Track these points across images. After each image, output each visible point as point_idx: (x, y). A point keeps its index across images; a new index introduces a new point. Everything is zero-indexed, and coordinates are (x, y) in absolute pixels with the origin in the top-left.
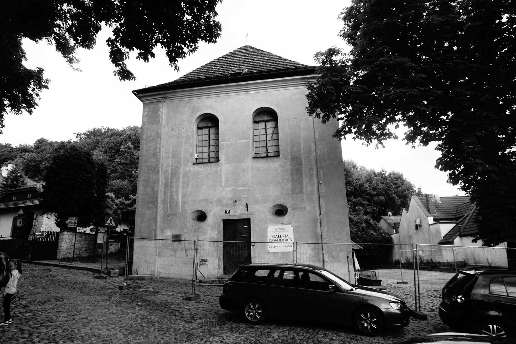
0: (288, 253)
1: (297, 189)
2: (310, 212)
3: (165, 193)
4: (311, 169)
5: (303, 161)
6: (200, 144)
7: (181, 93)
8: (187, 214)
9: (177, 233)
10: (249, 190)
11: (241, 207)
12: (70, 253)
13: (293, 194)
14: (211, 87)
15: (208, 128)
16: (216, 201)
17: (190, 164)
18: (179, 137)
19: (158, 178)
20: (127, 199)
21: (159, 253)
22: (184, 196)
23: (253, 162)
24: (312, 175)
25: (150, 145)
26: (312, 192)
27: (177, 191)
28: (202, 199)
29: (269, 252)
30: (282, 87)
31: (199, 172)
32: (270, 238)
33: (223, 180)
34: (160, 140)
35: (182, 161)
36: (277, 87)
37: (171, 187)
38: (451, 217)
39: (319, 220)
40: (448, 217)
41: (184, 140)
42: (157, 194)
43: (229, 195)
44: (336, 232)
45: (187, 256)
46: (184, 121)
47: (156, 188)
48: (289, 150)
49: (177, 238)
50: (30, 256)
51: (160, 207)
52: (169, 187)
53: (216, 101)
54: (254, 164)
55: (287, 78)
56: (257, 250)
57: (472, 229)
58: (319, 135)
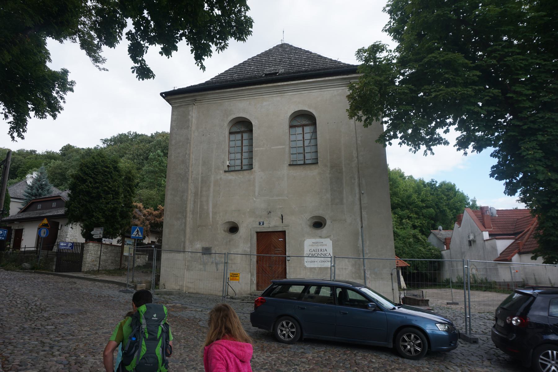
3: (195, 202)
5: (344, 170)
6: (232, 150)
7: (211, 95)
9: (207, 245)
12: (95, 265)
14: (244, 88)
17: (221, 172)
20: (156, 209)
29: (305, 267)
32: (306, 251)
33: (257, 189)
34: (190, 146)
36: (315, 88)
38: (509, 232)
39: (360, 234)
40: (505, 233)
45: (217, 270)
49: (207, 251)
50: (54, 267)
55: (327, 78)
57: (532, 246)
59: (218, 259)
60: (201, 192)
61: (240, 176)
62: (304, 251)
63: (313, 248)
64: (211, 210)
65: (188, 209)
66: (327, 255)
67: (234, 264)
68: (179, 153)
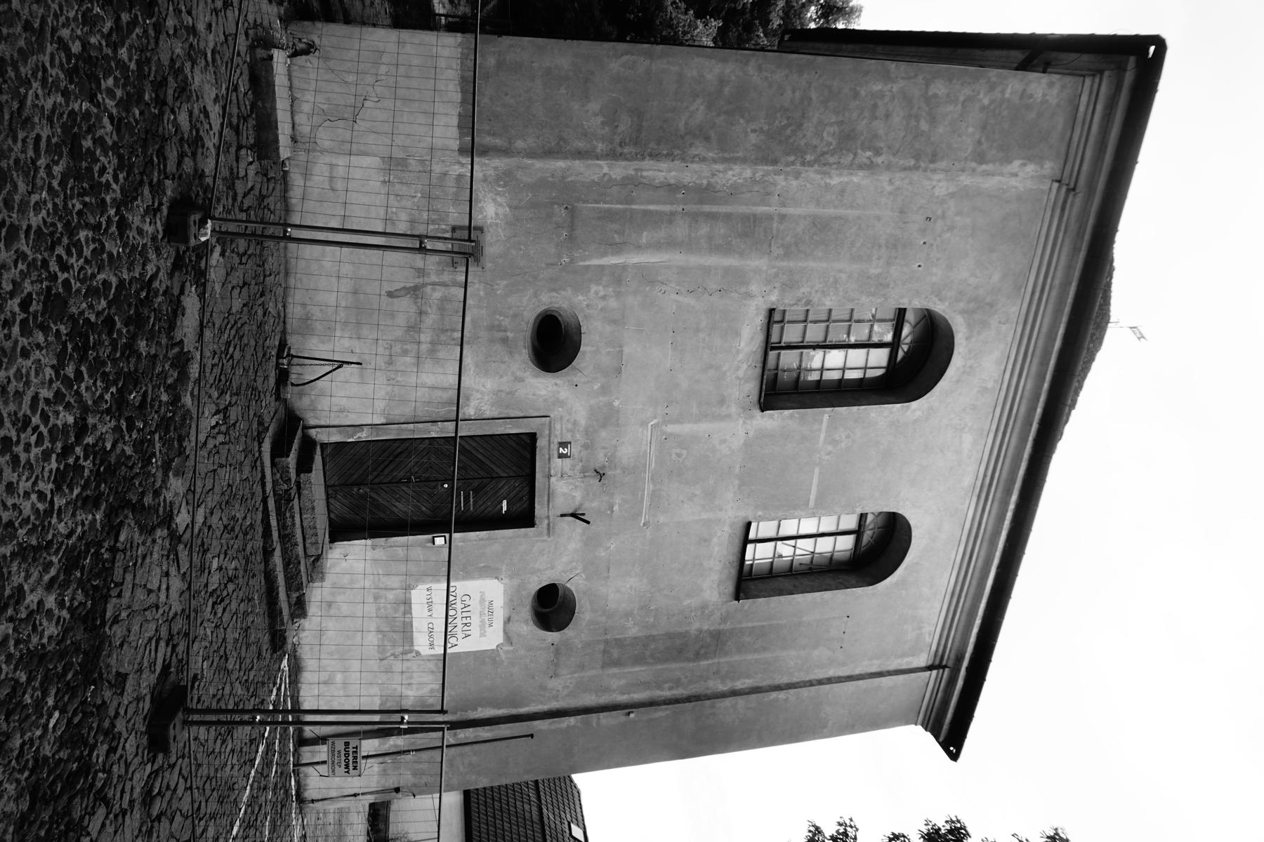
0: (410, 640)
1: (615, 652)
2: (543, 687)
3: (673, 189)
4: (677, 683)
5: (704, 663)
9: (493, 245)
11: (578, 495)
13: (607, 642)
14: (1046, 386)
16: (610, 404)
17: (773, 298)
18: (897, 245)
19: (744, 161)
21: (402, 163)
22: (647, 276)
23: (731, 526)
24: (659, 687)
26: (607, 690)
28: (626, 350)
29: (408, 588)
30: (956, 595)
31: (738, 334)
32: (459, 586)
33: (686, 428)
35: (792, 264)
37: (695, 217)
39: (514, 711)
41: (873, 271)
42: (670, 156)
43: (626, 453)
44: (474, 759)
45: (391, 295)
47: (699, 149)
48: (750, 625)
49: (466, 246)
51: (610, 167)
53: (984, 390)
54: (727, 529)
55: (978, 622)
56: (417, 553)
58: (777, 700)
59: (438, 294)
60: (712, 217)
61: (745, 366)
62: (464, 578)
63: (474, 604)
64: (635, 259)
65: (647, 163)
67: (418, 364)
68: (887, 116)
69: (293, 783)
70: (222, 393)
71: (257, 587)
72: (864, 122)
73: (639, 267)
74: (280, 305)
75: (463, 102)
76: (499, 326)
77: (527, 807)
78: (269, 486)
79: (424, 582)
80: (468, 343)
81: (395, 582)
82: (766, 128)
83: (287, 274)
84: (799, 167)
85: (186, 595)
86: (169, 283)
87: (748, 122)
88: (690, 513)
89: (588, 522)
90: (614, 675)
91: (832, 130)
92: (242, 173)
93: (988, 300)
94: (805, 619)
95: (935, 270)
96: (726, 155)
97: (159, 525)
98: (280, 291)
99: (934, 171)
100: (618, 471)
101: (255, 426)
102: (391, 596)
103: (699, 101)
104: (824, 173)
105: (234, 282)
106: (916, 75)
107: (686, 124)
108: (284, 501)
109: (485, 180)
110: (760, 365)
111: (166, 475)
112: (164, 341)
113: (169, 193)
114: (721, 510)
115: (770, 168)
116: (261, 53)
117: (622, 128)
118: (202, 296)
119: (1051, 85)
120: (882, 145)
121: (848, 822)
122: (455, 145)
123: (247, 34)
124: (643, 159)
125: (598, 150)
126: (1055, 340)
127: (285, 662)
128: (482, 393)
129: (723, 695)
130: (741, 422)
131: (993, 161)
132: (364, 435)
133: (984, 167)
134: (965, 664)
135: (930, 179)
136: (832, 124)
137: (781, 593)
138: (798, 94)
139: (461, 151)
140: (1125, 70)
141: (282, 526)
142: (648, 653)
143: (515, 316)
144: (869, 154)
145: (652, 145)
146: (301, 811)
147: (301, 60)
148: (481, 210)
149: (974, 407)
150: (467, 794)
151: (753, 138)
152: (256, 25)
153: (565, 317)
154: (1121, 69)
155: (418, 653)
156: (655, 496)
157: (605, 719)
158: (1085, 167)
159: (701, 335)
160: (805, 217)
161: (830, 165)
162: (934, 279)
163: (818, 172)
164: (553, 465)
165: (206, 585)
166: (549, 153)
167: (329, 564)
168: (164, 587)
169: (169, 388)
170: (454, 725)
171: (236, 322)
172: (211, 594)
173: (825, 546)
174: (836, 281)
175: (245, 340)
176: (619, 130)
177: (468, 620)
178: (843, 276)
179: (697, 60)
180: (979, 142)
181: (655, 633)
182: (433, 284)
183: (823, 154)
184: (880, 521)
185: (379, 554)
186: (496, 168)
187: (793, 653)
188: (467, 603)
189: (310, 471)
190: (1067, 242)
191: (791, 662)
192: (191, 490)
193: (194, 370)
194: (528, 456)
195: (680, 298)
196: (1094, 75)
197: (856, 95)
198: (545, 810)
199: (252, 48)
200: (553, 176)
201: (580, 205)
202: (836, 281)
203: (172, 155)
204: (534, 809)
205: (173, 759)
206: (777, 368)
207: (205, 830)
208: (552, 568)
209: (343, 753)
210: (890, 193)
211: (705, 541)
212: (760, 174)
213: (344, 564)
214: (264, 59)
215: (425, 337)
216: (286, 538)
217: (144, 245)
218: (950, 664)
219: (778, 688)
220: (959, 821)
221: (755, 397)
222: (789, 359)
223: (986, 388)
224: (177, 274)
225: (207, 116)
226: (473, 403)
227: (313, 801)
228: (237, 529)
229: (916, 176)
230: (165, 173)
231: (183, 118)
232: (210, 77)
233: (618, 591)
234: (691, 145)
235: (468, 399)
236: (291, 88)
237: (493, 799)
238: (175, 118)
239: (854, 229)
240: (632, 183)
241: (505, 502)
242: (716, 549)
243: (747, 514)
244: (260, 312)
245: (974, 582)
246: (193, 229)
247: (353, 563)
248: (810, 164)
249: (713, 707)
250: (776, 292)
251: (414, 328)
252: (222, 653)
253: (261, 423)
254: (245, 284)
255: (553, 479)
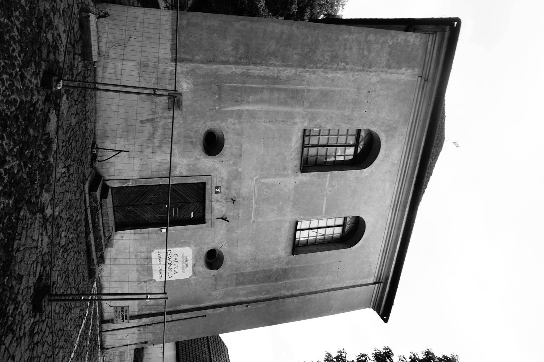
1: (242, 278)
4: (268, 292)
5: (279, 283)
7: (426, 110)
8: (219, 122)
9: (186, 102)
10: (251, 218)
11: (224, 210)
13: (237, 274)
14: (419, 162)
15: (356, 146)
16: (237, 170)
17: (306, 125)
18: (356, 103)
19: (292, 66)
21: (147, 66)
22: (252, 115)
24: (260, 294)
25: (355, 50)
27: (262, 101)
28: (244, 146)
29: (151, 251)
30: (385, 251)
31: (291, 140)
32: (173, 251)
33: (270, 180)
34: (358, 71)
35: (313, 110)
37: (272, 90)
39: (197, 306)
42: (261, 64)
43: (244, 191)
44: (180, 327)
45: (142, 122)
46: (378, 112)
47: (273, 61)
48: (299, 266)
51: (236, 68)
52: (272, 86)
53: (394, 164)
54: (288, 224)
55: (394, 262)
56: (154, 236)
60: (279, 90)
61: (294, 154)
63: (179, 258)
64: (247, 107)
65: (252, 67)
66: (170, 275)
68: (351, 49)
69: (99, 339)
70: (67, 159)
71: (82, 248)
72: (341, 51)
73: (248, 111)
74: (93, 126)
75: (173, 40)
76: (189, 136)
77: (204, 356)
78: (88, 204)
79: (157, 249)
80: (176, 143)
81: (144, 249)
82: (301, 52)
83: (96, 113)
84: (315, 69)
85: (50, 245)
86: (43, 107)
87: (293, 50)
88: (272, 217)
89: (228, 221)
90: (241, 289)
91: (328, 54)
92: (76, 65)
93: (394, 126)
94: (322, 263)
95: (372, 113)
96: (285, 64)
97: (38, 212)
98: (93, 120)
99: (371, 72)
100: (241, 199)
101: (81, 177)
102: (142, 255)
103: (273, 41)
104: (325, 72)
105: (72, 112)
106: (362, 32)
107: (267, 50)
108: (94, 211)
109: (182, 73)
110: (300, 153)
111: (41, 192)
112: (41, 131)
113: (43, 67)
114: (285, 216)
115: (303, 69)
116: (84, 14)
117: (240, 51)
118: (58, 115)
119: (416, 37)
120: (349, 60)
121: (342, 350)
122: (169, 57)
123: (78, 6)
124: (250, 65)
125: (231, 61)
126: (422, 142)
127: (95, 285)
128: (182, 165)
129: (288, 297)
130: (293, 177)
131: (394, 68)
132: (130, 184)
133: (391, 70)
134: (389, 281)
135: (369, 75)
136: (328, 52)
137: (311, 252)
138: (314, 39)
139: (172, 60)
140: (445, 31)
141: (94, 222)
142: (255, 279)
143: (196, 132)
144: (343, 64)
145: (253, 59)
146: (102, 353)
147: (102, 20)
148: (181, 86)
149: (390, 171)
150: (177, 344)
151: (296, 57)
152: (82, 3)
153: (217, 133)
154: (444, 31)
155: (155, 281)
156: (257, 210)
157: (237, 308)
158: (431, 71)
159: (275, 140)
160: (318, 91)
161: (328, 68)
162: (372, 117)
163: (323, 72)
164: (213, 197)
165: (59, 243)
166: (210, 62)
167: (115, 241)
168: (40, 239)
169: (43, 153)
170: (169, 313)
171: (73, 129)
172: (62, 247)
173: (329, 231)
174: (331, 118)
175: (77, 138)
176: (239, 52)
177: (177, 266)
178: (334, 115)
179: (272, 24)
180: (388, 60)
181: (258, 270)
182: (160, 118)
183: (325, 64)
184: (352, 221)
185: (137, 236)
186: (187, 68)
187: (317, 278)
188: (176, 258)
189: (106, 198)
190: (425, 102)
191: (317, 282)
192: (53, 199)
193: (54, 147)
194: (202, 193)
195: (266, 124)
196: (433, 34)
197: (338, 40)
198: (212, 357)
199: (80, 12)
200: (211, 72)
201: (223, 84)
202: (331, 118)
203: (45, 51)
204: (208, 357)
205: (44, 318)
206: (308, 155)
207: (58, 353)
208: (213, 242)
209: (121, 312)
210: (353, 81)
211: (279, 229)
212: (298, 72)
213: (121, 241)
214: (85, 17)
215: (157, 142)
216: (96, 228)
217: (32, 88)
218: (383, 281)
219: (311, 293)
220: (389, 349)
221: (298, 167)
222: (313, 151)
223: (395, 163)
224: (47, 103)
225: (60, 37)
226: (178, 170)
227: (108, 349)
228: (73, 220)
229: (363, 74)
230: (42, 58)
231: (50, 36)
232: (62, 21)
233: (242, 252)
234: (270, 59)
235: (176, 167)
236: (97, 31)
237: (189, 352)
238: (46, 36)
239: (338, 96)
240: (246, 75)
241: (192, 213)
242: (284, 233)
243: (297, 217)
244: (84, 127)
245: (392, 246)
246: (54, 84)
247: (125, 241)
248: (319, 68)
249: (283, 302)
250: (307, 122)
251: (152, 137)
252: (66, 274)
253: (84, 176)
254: (77, 113)
255: (213, 203)
